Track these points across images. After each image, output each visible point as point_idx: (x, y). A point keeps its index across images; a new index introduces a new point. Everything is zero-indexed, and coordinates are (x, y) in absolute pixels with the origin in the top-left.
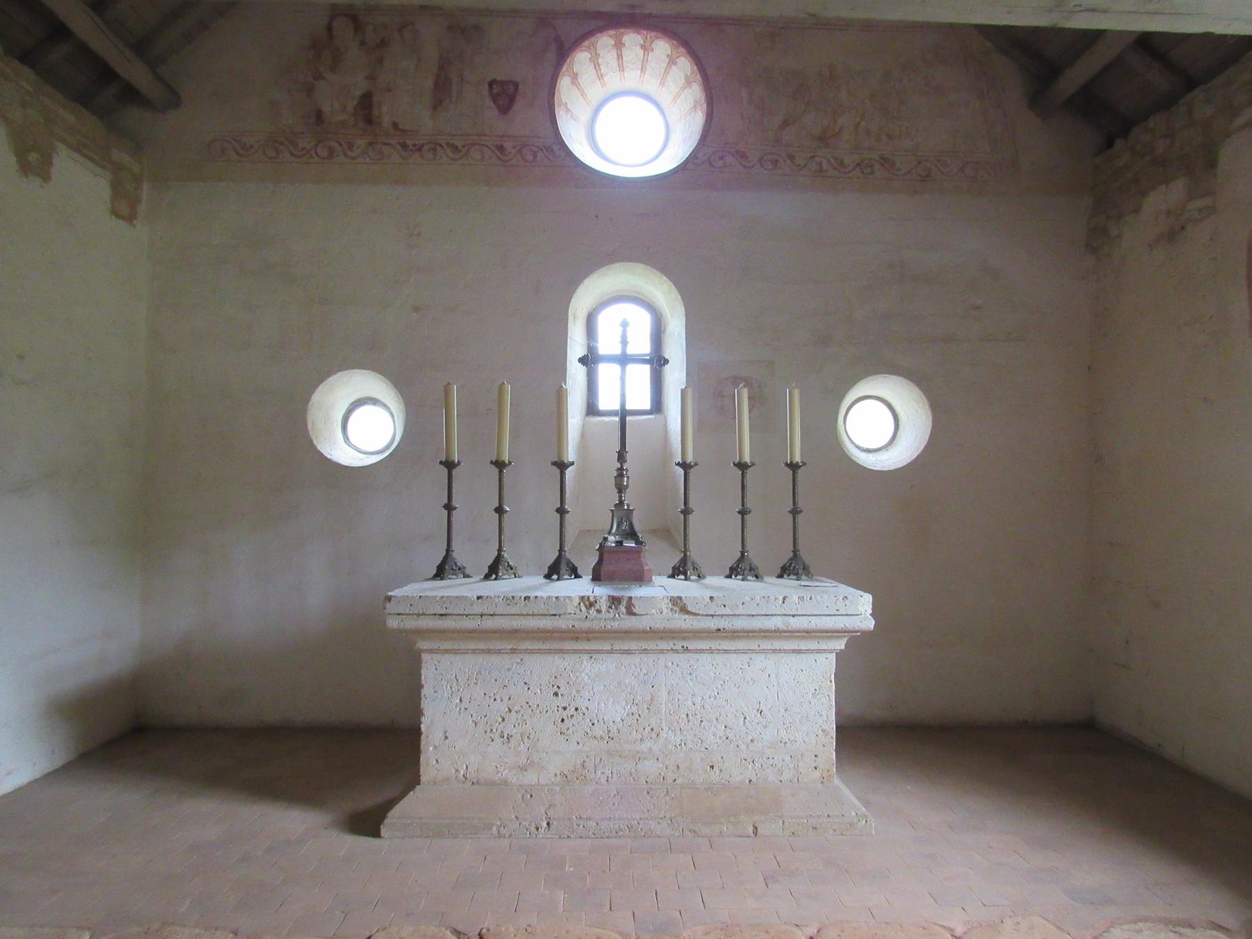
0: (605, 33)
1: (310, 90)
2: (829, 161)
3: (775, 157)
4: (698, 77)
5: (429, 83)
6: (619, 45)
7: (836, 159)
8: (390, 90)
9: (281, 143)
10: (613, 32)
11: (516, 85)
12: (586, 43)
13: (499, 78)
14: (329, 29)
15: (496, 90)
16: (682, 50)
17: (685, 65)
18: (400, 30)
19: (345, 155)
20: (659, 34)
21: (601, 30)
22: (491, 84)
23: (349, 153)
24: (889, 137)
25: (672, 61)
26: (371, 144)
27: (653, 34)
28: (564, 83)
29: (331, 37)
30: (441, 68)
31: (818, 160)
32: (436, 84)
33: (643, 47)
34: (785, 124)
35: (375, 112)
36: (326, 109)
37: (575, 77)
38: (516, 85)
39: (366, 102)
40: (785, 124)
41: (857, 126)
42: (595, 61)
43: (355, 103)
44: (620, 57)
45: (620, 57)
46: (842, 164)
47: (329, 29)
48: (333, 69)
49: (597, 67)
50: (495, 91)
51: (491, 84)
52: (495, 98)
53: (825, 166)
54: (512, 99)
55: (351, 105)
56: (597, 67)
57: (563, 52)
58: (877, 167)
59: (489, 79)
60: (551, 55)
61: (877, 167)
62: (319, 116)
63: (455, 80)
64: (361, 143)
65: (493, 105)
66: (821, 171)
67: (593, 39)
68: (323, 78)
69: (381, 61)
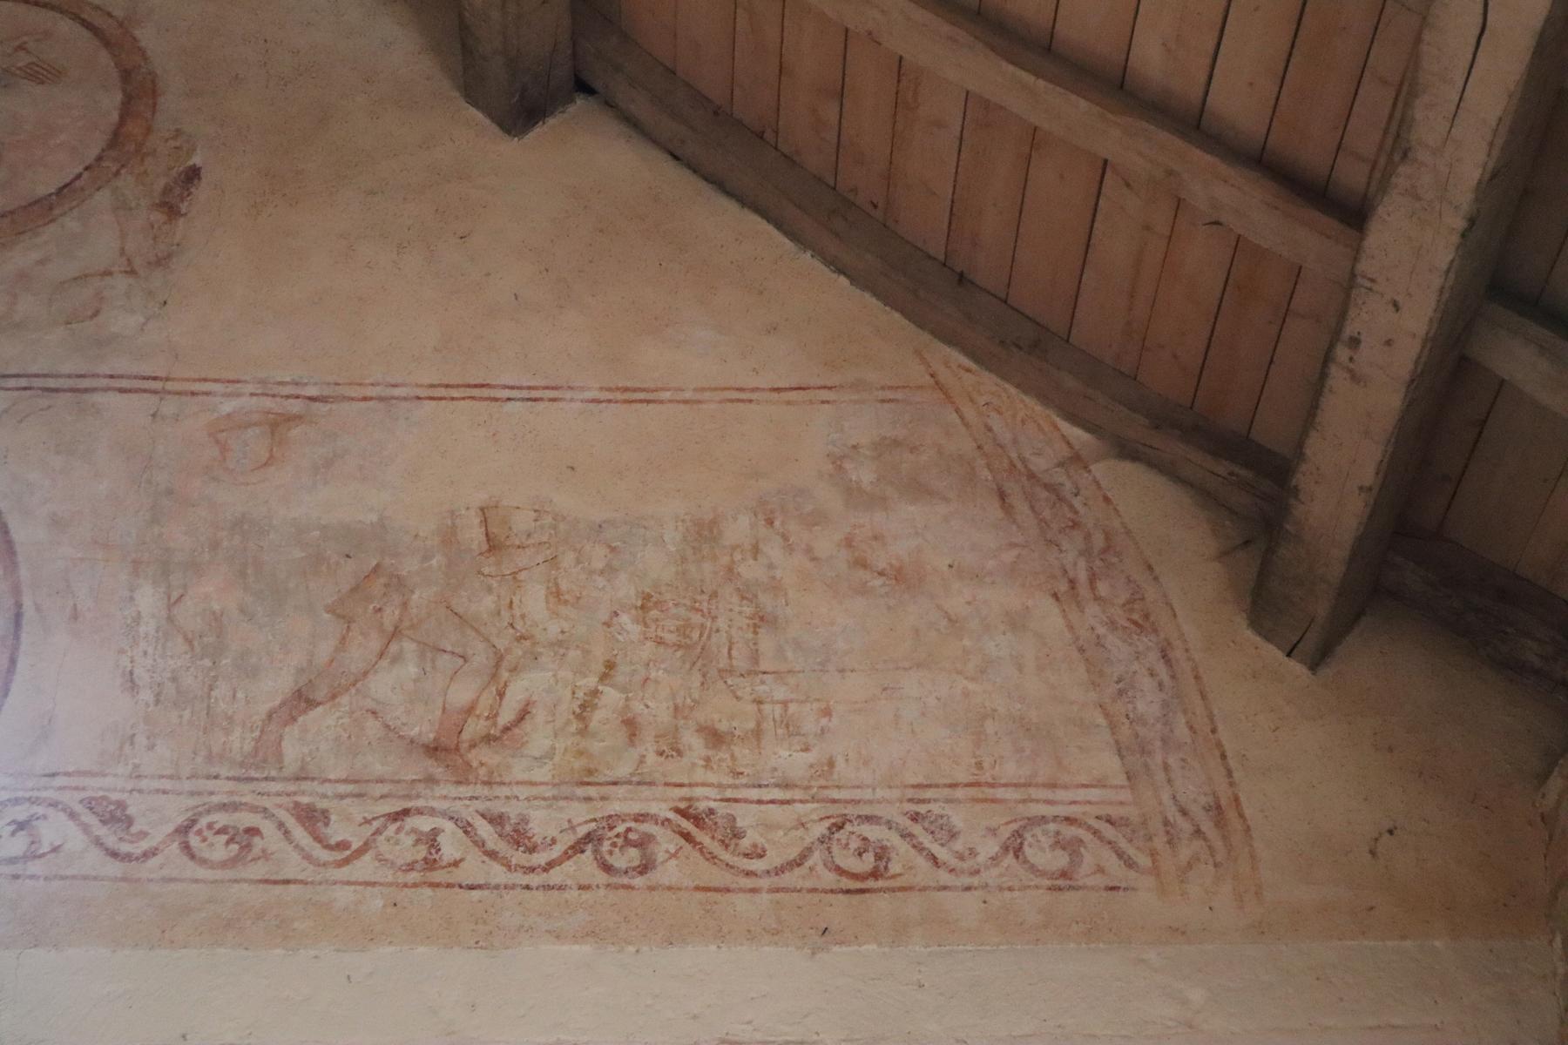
2: (467, 828)
3: (246, 819)
7: (497, 820)
24: (715, 738)
31: (425, 824)
34: (302, 700)
40: (302, 700)
41: (586, 708)
46: (520, 838)
53: (449, 851)
58: (666, 842)
61: (666, 842)
66: (430, 864)
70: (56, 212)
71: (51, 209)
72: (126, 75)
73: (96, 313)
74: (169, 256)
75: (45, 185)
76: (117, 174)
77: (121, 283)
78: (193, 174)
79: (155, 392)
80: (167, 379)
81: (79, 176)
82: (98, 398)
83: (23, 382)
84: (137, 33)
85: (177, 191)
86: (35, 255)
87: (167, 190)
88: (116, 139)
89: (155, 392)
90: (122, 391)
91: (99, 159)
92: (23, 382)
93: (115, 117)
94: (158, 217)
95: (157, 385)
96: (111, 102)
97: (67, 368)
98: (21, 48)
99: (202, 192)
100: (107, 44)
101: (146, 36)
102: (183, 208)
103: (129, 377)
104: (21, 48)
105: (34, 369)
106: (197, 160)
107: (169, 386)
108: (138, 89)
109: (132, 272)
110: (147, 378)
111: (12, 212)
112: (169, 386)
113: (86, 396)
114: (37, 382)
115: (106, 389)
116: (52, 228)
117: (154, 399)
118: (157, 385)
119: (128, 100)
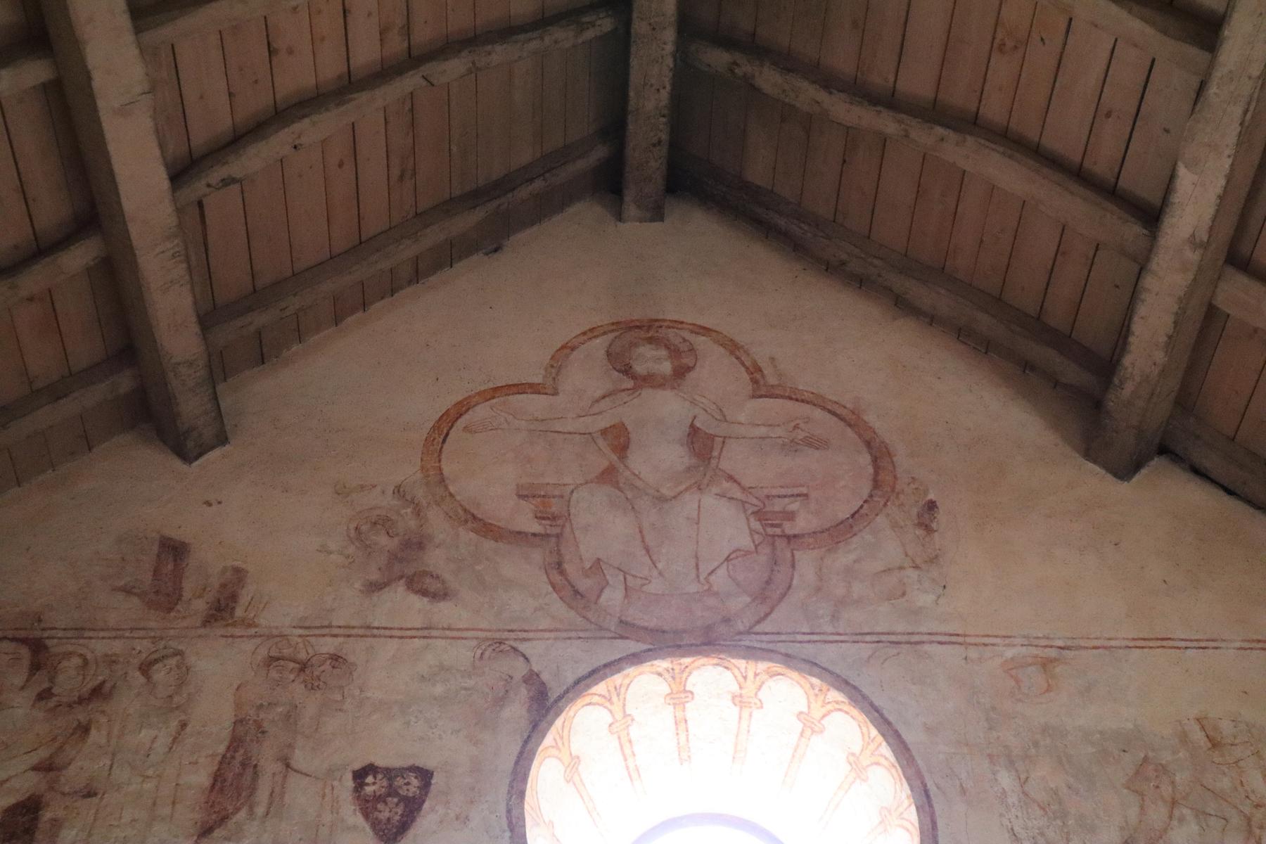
0: (646, 667)
4: (886, 750)
5: (201, 778)
6: (680, 696)
8: (90, 794)
10: (663, 664)
11: (425, 775)
12: (601, 688)
13: (380, 762)
15: (373, 786)
16: (835, 695)
17: (847, 729)
18: (145, 669)
20: (778, 668)
21: (636, 659)
22: (360, 776)
25: (810, 726)
27: (762, 666)
28: (546, 774)
30: (236, 742)
32: (218, 777)
33: (739, 700)
37: (574, 763)
38: (425, 775)
42: (621, 726)
44: (681, 723)
45: (681, 723)
49: (625, 746)
50: (369, 790)
51: (360, 776)
52: (367, 806)
54: (412, 807)
56: (625, 746)
57: (544, 704)
59: (357, 766)
60: (517, 710)
63: (269, 768)
65: (359, 820)
67: (618, 679)
69: (84, 729)
70: (855, 529)
71: (851, 527)
72: (868, 444)
73: (904, 594)
74: (937, 557)
75: (844, 512)
76: (885, 505)
77: (912, 574)
78: (932, 506)
79: (960, 644)
80: (965, 636)
81: (862, 507)
82: (926, 647)
83: (875, 638)
84: (866, 418)
85: (926, 516)
86: (852, 557)
87: (919, 516)
88: (876, 484)
89: (960, 644)
90: (940, 643)
91: (871, 496)
92: (875, 638)
93: (871, 470)
94: (920, 532)
95: (960, 639)
96: (865, 459)
97: (900, 628)
98: (796, 427)
99: (942, 516)
100: (850, 425)
101: (870, 418)
102: (934, 525)
103: (940, 634)
104: (796, 427)
105: (879, 629)
106: (931, 496)
107: (968, 640)
108: (880, 455)
109: (916, 567)
110: (951, 635)
111: (828, 530)
112: (968, 640)
113: (918, 647)
114: (883, 638)
115: (931, 642)
116: (855, 539)
117: (963, 648)
118: (960, 639)
119: (875, 461)
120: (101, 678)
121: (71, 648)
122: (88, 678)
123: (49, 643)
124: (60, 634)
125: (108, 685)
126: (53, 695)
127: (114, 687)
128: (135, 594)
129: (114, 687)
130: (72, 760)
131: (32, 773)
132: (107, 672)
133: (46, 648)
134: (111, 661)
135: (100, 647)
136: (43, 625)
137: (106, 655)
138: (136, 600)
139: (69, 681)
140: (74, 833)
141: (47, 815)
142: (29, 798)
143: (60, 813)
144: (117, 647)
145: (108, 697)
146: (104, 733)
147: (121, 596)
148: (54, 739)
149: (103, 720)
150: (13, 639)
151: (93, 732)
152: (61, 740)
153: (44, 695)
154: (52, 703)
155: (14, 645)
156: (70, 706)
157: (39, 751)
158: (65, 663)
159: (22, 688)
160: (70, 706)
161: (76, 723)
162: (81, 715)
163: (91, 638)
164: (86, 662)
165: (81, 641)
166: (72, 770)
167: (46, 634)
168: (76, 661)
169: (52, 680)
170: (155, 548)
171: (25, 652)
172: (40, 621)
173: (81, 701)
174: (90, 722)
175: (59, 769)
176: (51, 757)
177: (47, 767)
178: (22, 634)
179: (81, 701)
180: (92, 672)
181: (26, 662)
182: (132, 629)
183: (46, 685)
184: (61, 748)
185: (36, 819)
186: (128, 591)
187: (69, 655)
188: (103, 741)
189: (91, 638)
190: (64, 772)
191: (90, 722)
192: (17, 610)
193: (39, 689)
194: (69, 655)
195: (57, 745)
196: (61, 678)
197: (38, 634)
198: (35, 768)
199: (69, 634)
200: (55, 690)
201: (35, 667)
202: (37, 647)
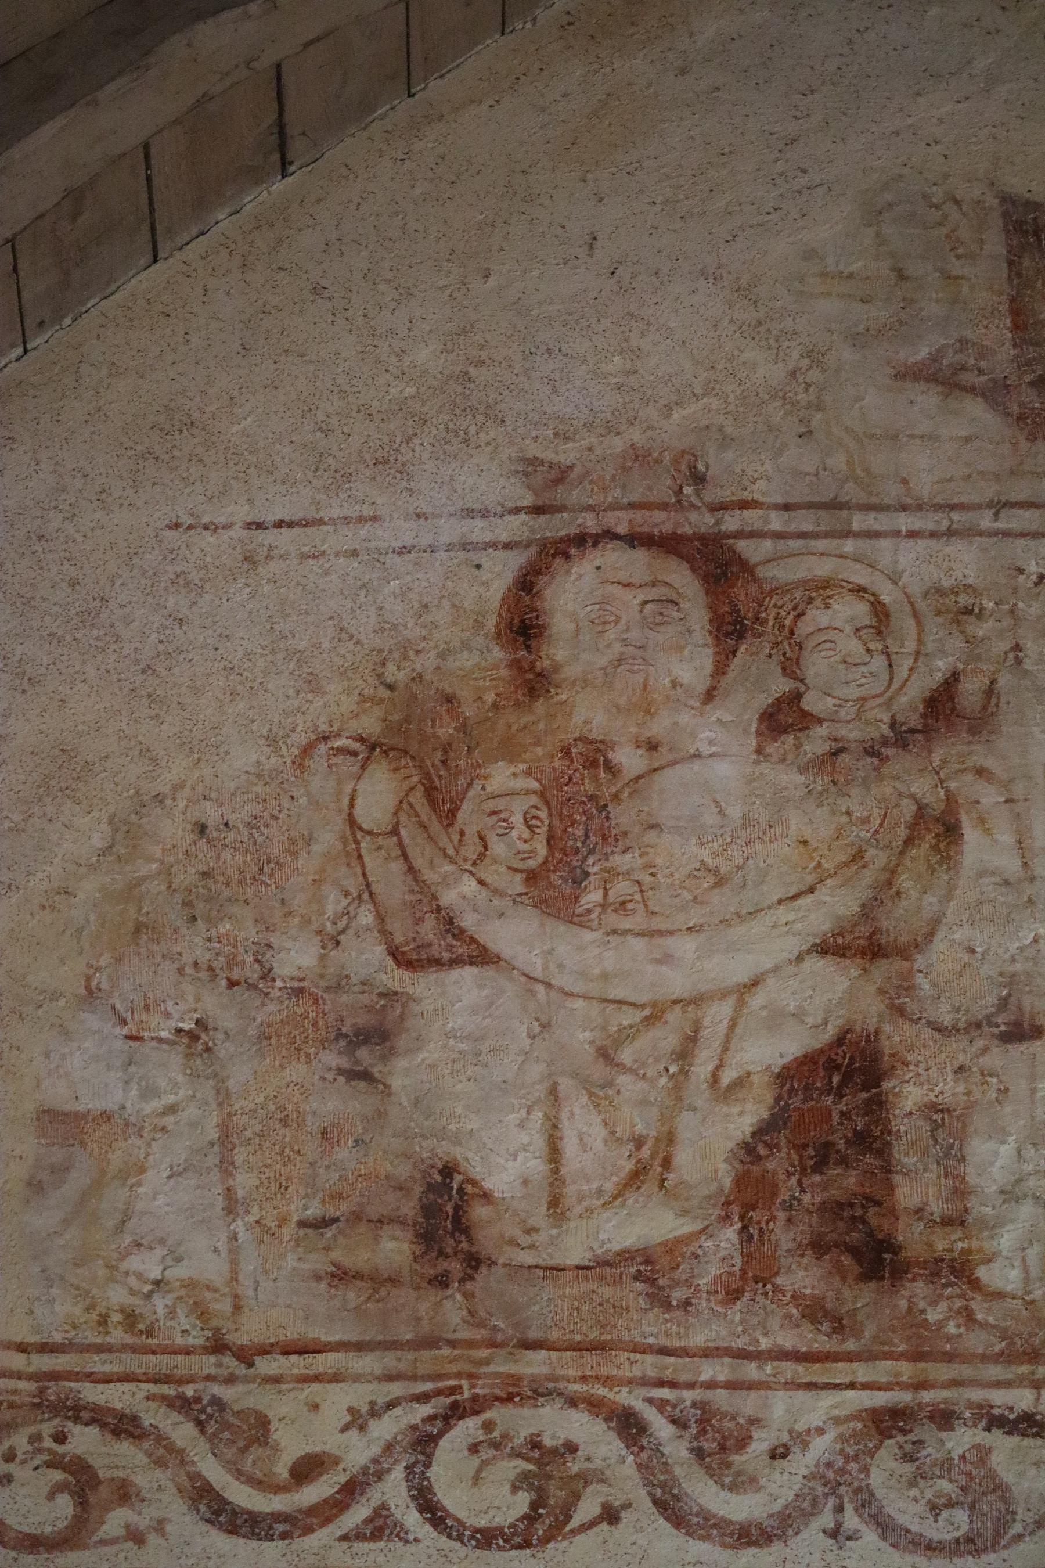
1: (371, 1038)
9: (123, 1426)
14: (523, 626)
19: (670, 1506)
23: (705, 1493)
26: (887, 1423)
29: (534, 682)
35: (917, 1188)
36: (505, 1165)
39: (837, 1105)
43: (745, 1118)
47: (523, 626)
48: (555, 884)
55: (713, 1139)
62: (446, 1216)
64: (813, 1415)
68: (483, 957)
69: (940, 829)
120: (942, 665)
121: (823, 568)
122: (902, 673)
123: (751, 550)
124: (776, 522)
125: (971, 688)
126: (806, 720)
127: (990, 692)
128: (972, 390)
129: (990, 692)
130: (936, 923)
131: (815, 964)
132: (957, 643)
133: (746, 567)
134: (960, 610)
135: (911, 565)
136: (713, 494)
137: (940, 592)
138: (976, 407)
139: (846, 675)
140: (1007, 1150)
141: (909, 1095)
142: (840, 1040)
143: (950, 1090)
144: (965, 562)
145: (982, 723)
146: (1007, 838)
147: (928, 398)
148: (857, 856)
149: (990, 797)
150: (634, 540)
151: (970, 834)
152: (877, 858)
153: (785, 718)
154: (816, 741)
155: (641, 555)
156: (871, 751)
157: (823, 894)
158: (817, 617)
159: (709, 696)
160: (871, 751)
161: (908, 809)
162: (915, 782)
163: (877, 535)
164: (880, 612)
165: (849, 546)
166: (941, 956)
167: (731, 522)
168: (848, 611)
169: (791, 667)
170: (995, 244)
171: (681, 578)
172: (699, 479)
173: (901, 737)
174: (950, 799)
175: (904, 952)
176: (867, 912)
177: (859, 944)
178: (661, 522)
179: (901, 737)
180: (910, 646)
181: (696, 613)
182: (999, 506)
183: (780, 686)
184: (887, 886)
185: (877, 1106)
186: (944, 378)
187: (822, 589)
188: (1011, 865)
189: (877, 535)
190: (920, 962)
191: (950, 799)
192: (618, 444)
193: (763, 701)
194: (822, 589)
195: (869, 876)
196: (817, 666)
197: (701, 521)
198: (824, 949)
199: (805, 521)
200: (811, 702)
201: (730, 630)
202: (717, 564)
